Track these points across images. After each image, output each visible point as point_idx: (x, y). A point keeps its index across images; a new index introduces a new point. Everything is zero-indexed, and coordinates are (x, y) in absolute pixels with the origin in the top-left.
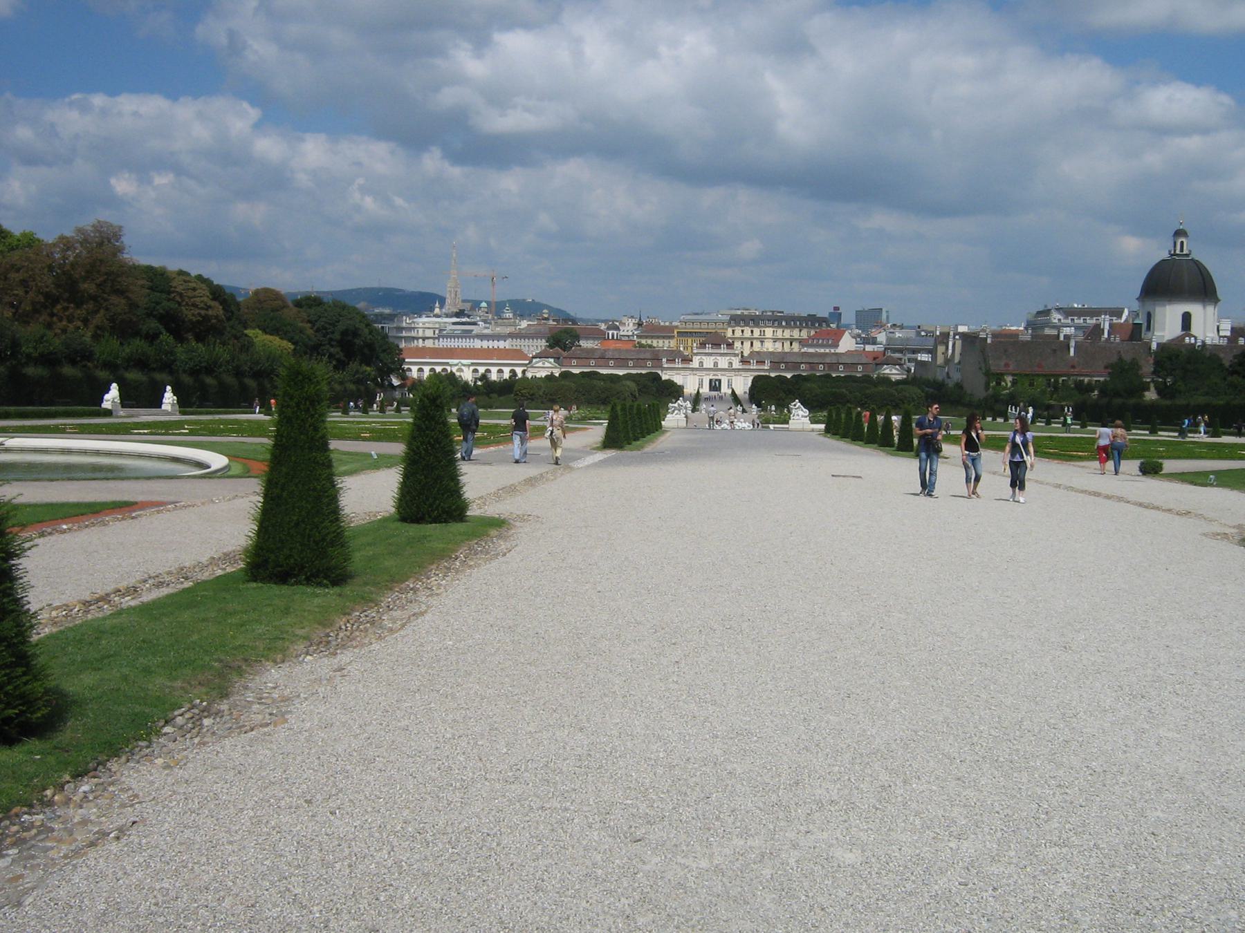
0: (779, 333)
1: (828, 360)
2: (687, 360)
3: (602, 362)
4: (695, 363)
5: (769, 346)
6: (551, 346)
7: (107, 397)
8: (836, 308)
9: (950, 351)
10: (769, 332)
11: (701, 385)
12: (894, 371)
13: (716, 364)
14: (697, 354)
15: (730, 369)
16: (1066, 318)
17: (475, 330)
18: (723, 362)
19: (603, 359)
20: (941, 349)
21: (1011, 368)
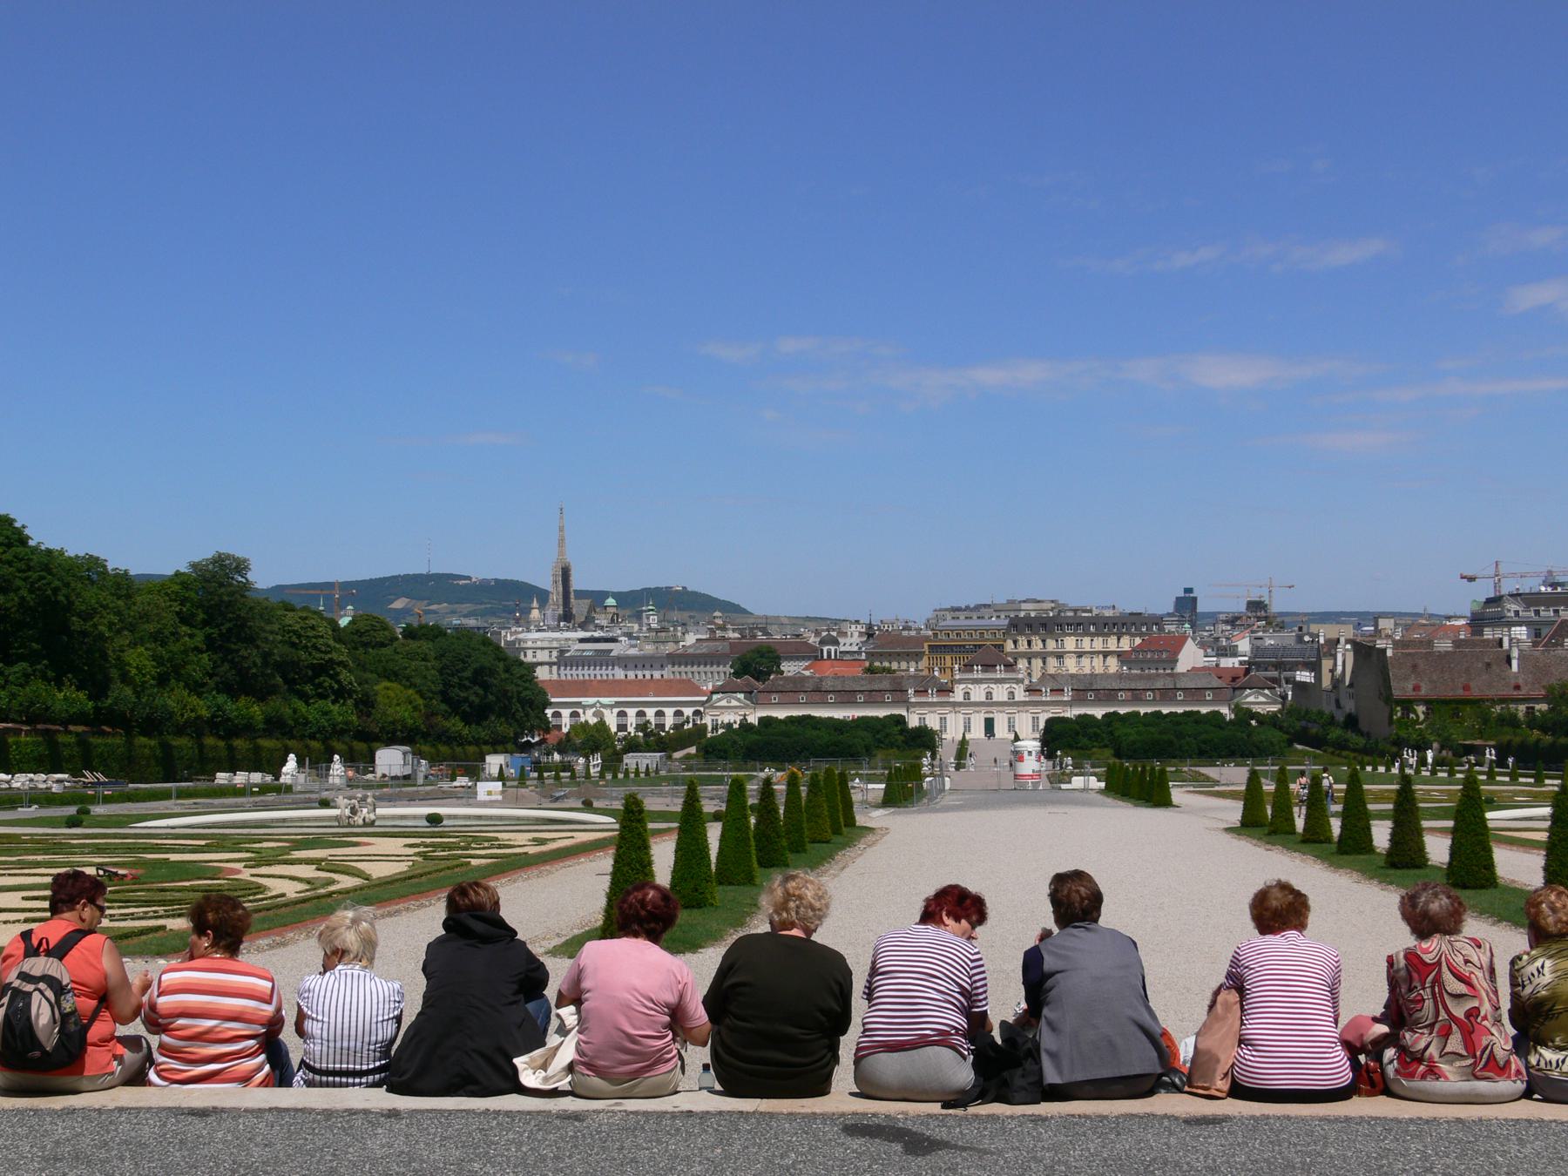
0: (1086, 644)
1: (1159, 685)
2: (946, 690)
3: (817, 697)
4: (958, 695)
5: (1071, 665)
6: (737, 674)
7: (284, 769)
8: (1188, 590)
9: (1339, 668)
10: (1070, 643)
11: (967, 728)
12: (1262, 699)
13: (989, 695)
14: (960, 681)
15: (1011, 702)
16: (1527, 609)
17: (616, 649)
18: (1000, 693)
19: (818, 693)
20: (1326, 664)
21: (1423, 692)
